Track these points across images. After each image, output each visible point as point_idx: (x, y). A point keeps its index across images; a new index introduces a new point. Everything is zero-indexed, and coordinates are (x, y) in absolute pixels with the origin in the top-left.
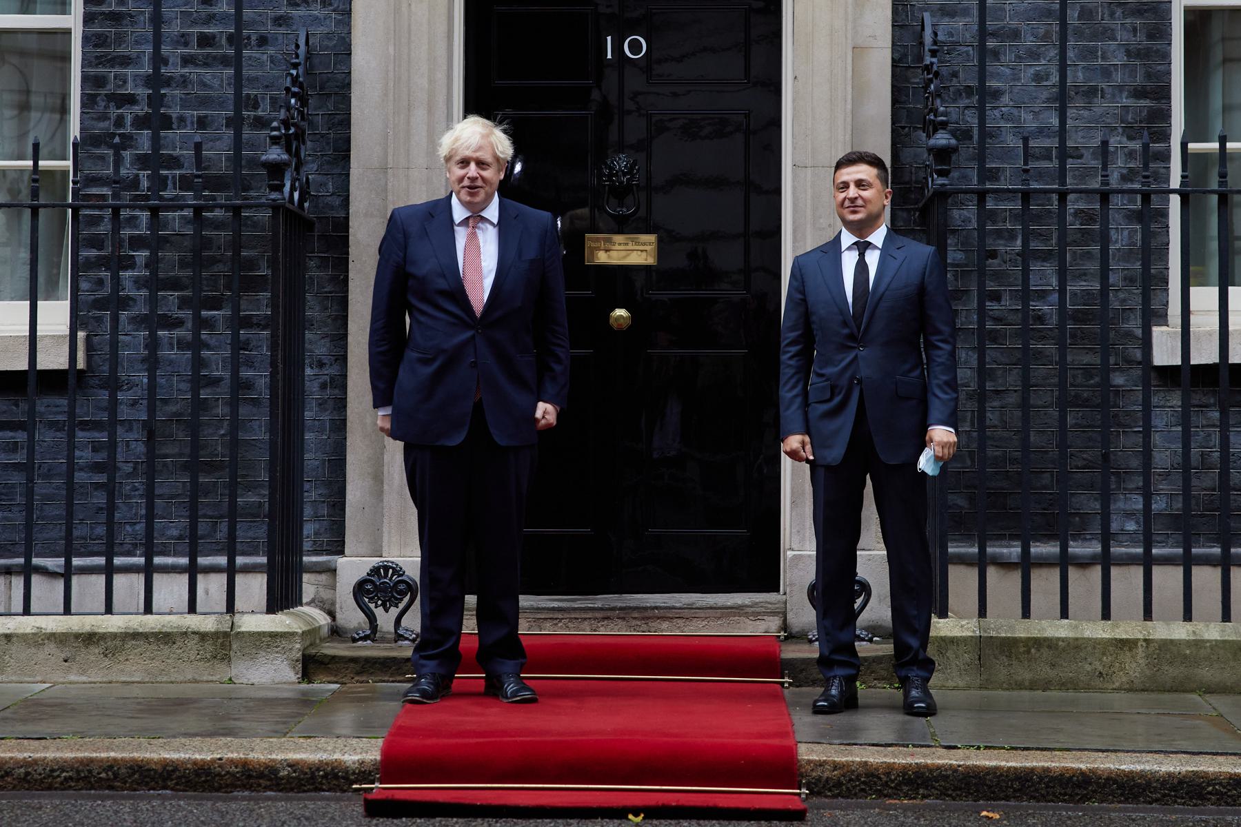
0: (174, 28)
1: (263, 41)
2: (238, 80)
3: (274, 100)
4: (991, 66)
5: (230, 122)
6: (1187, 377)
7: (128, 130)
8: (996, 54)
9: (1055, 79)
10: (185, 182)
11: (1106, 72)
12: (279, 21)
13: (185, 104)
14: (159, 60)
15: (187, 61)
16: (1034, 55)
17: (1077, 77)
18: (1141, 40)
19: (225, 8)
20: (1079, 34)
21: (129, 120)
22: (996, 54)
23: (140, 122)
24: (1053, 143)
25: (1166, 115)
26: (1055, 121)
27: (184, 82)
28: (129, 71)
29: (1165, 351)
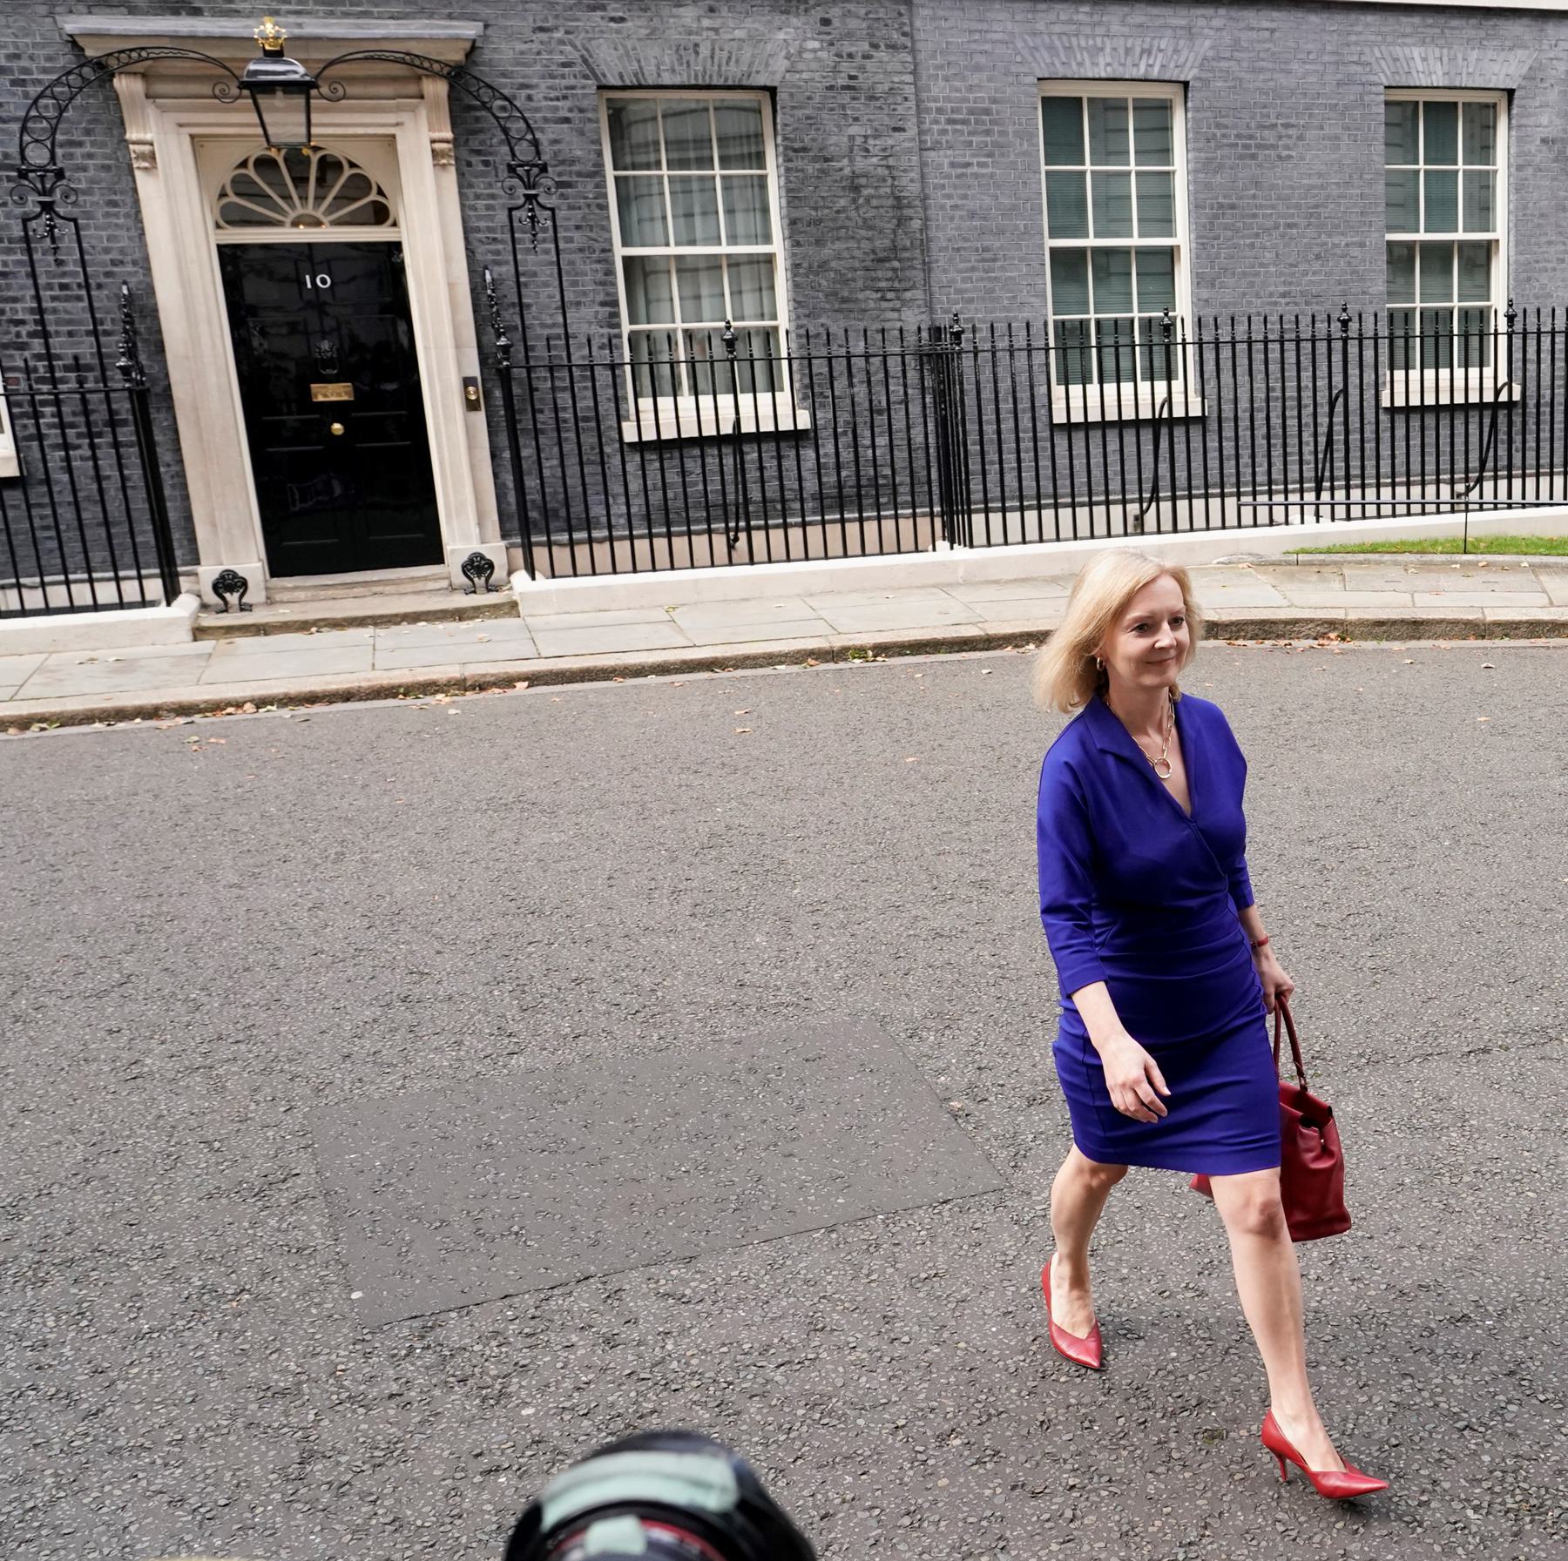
0: (42, 281)
1: (99, 286)
2: (92, 309)
3: (113, 320)
4: (524, 291)
5: (88, 333)
6: (641, 446)
7: (25, 339)
8: (526, 285)
9: (558, 297)
10: (67, 369)
11: (585, 294)
12: (108, 274)
13: (58, 323)
14: (38, 298)
15: (54, 299)
16: (546, 285)
17: (569, 296)
18: (600, 276)
19: (70, 268)
20: (568, 273)
21: (24, 333)
22: (526, 285)
23: (31, 335)
24: (561, 331)
25: (617, 315)
26: (561, 319)
27: (55, 311)
28: (18, 306)
29: (630, 435)
